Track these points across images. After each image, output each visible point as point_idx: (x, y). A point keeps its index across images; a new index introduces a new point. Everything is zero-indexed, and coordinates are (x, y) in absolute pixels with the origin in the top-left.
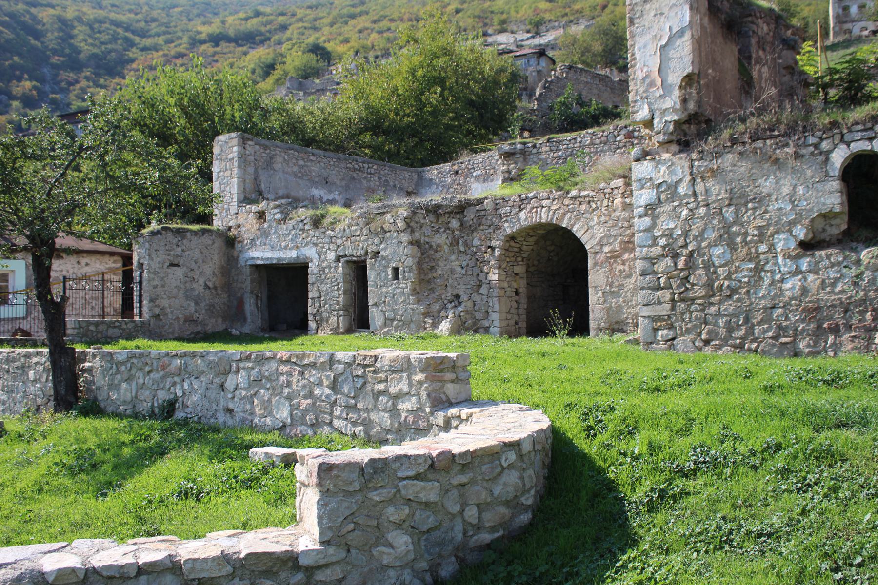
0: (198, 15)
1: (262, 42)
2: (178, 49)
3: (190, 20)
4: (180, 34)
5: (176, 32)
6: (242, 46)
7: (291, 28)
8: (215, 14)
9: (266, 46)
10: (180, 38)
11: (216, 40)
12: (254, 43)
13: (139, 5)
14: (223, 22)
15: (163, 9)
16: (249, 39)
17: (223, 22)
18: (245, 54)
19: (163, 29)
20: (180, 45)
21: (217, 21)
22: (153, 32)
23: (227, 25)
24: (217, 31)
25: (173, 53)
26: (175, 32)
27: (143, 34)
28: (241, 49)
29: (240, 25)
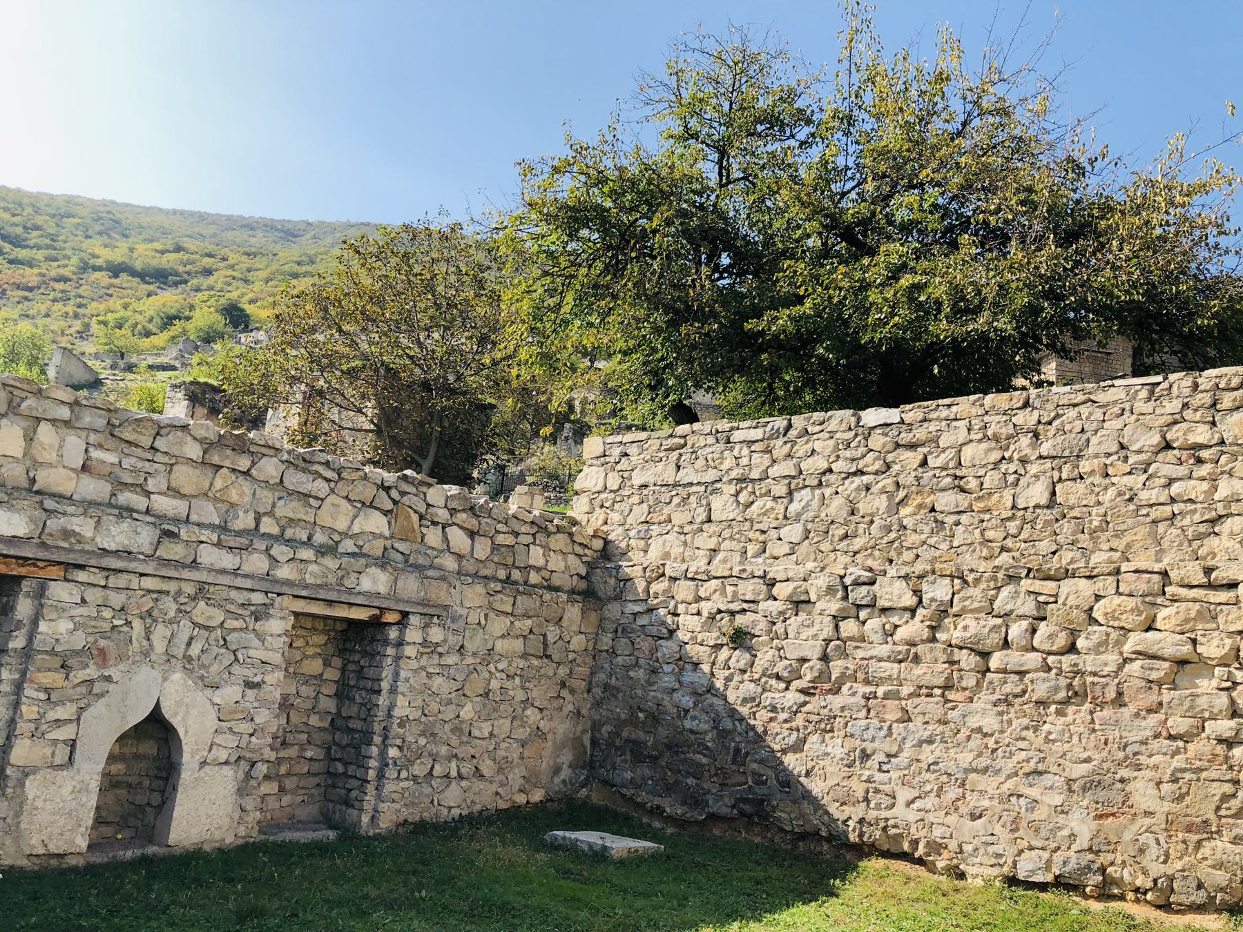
0: (100, 233)
1: (176, 284)
2: (61, 271)
3: (87, 237)
4: (69, 252)
5: (63, 249)
6: (150, 283)
7: (216, 274)
8: (126, 236)
9: (180, 290)
10: (69, 258)
11: (116, 270)
12: (165, 284)
13: (20, 205)
14: (131, 250)
15: (53, 216)
16: (161, 277)
17: (131, 250)
18: (149, 295)
19: (48, 241)
20: (65, 266)
21: (123, 245)
22: (31, 243)
23: (135, 255)
24: (120, 260)
25: (53, 274)
26: (63, 249)
27: (17, 242)
28: (146, 286)
29: (154, 257)
